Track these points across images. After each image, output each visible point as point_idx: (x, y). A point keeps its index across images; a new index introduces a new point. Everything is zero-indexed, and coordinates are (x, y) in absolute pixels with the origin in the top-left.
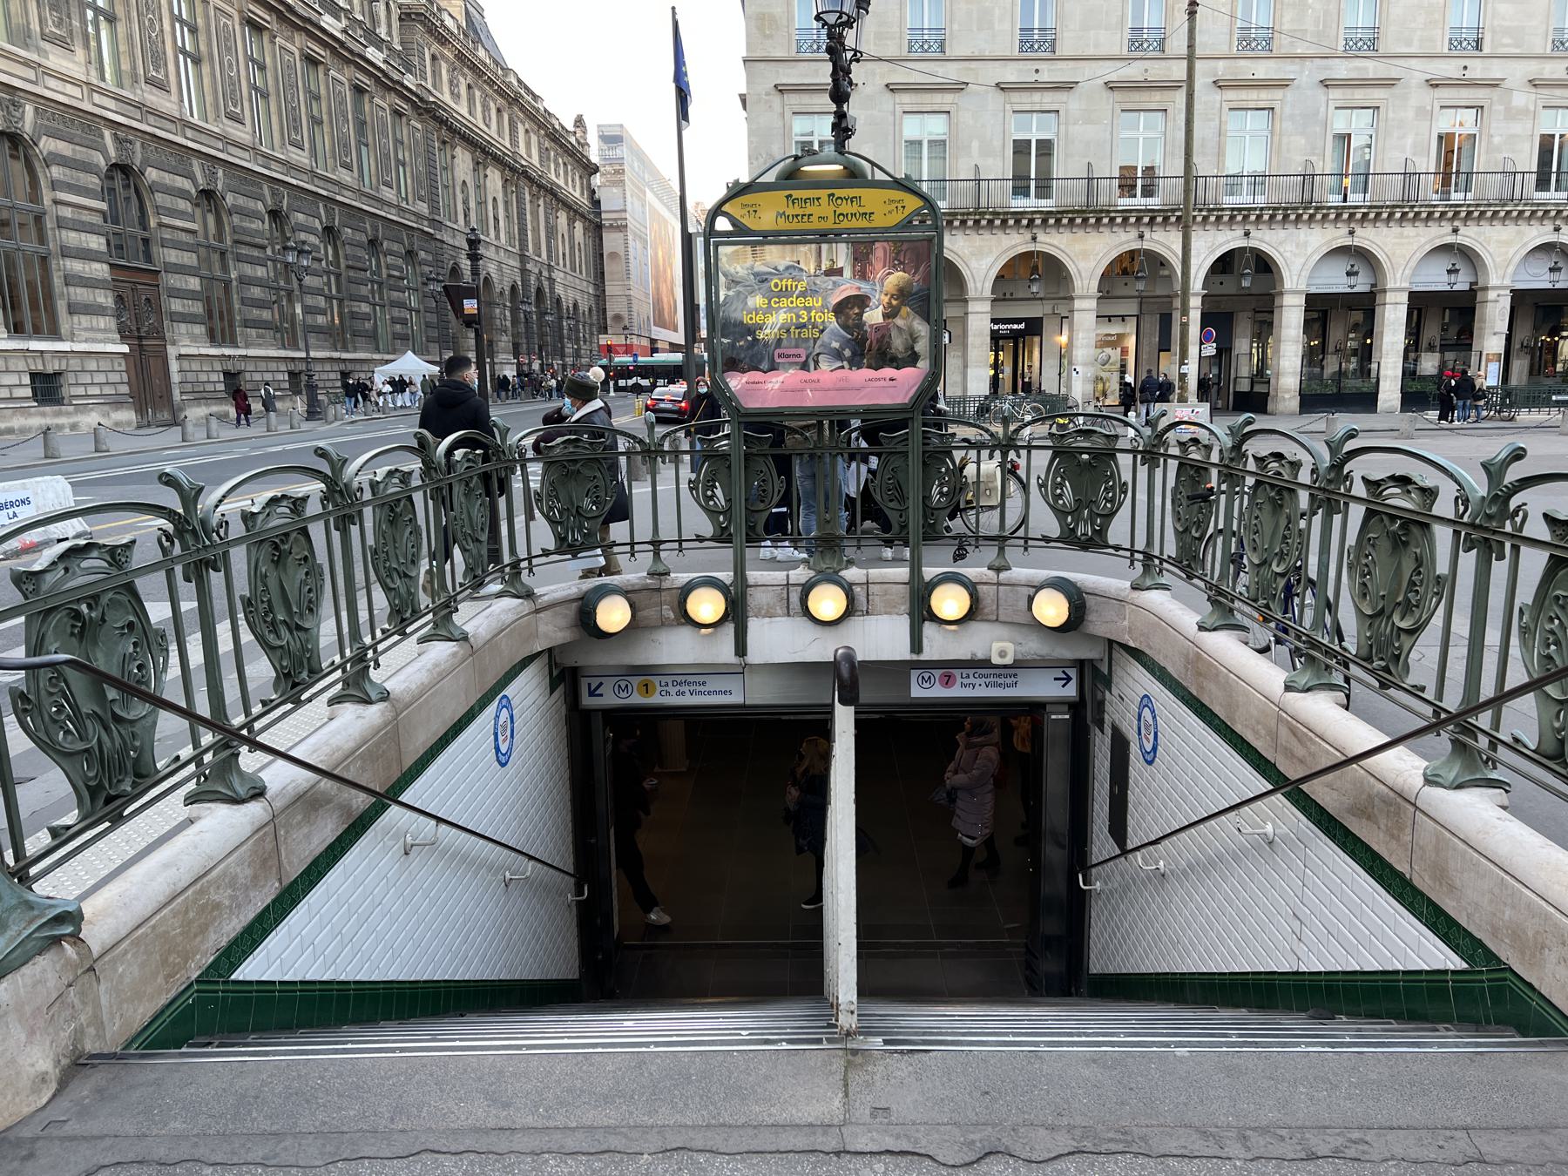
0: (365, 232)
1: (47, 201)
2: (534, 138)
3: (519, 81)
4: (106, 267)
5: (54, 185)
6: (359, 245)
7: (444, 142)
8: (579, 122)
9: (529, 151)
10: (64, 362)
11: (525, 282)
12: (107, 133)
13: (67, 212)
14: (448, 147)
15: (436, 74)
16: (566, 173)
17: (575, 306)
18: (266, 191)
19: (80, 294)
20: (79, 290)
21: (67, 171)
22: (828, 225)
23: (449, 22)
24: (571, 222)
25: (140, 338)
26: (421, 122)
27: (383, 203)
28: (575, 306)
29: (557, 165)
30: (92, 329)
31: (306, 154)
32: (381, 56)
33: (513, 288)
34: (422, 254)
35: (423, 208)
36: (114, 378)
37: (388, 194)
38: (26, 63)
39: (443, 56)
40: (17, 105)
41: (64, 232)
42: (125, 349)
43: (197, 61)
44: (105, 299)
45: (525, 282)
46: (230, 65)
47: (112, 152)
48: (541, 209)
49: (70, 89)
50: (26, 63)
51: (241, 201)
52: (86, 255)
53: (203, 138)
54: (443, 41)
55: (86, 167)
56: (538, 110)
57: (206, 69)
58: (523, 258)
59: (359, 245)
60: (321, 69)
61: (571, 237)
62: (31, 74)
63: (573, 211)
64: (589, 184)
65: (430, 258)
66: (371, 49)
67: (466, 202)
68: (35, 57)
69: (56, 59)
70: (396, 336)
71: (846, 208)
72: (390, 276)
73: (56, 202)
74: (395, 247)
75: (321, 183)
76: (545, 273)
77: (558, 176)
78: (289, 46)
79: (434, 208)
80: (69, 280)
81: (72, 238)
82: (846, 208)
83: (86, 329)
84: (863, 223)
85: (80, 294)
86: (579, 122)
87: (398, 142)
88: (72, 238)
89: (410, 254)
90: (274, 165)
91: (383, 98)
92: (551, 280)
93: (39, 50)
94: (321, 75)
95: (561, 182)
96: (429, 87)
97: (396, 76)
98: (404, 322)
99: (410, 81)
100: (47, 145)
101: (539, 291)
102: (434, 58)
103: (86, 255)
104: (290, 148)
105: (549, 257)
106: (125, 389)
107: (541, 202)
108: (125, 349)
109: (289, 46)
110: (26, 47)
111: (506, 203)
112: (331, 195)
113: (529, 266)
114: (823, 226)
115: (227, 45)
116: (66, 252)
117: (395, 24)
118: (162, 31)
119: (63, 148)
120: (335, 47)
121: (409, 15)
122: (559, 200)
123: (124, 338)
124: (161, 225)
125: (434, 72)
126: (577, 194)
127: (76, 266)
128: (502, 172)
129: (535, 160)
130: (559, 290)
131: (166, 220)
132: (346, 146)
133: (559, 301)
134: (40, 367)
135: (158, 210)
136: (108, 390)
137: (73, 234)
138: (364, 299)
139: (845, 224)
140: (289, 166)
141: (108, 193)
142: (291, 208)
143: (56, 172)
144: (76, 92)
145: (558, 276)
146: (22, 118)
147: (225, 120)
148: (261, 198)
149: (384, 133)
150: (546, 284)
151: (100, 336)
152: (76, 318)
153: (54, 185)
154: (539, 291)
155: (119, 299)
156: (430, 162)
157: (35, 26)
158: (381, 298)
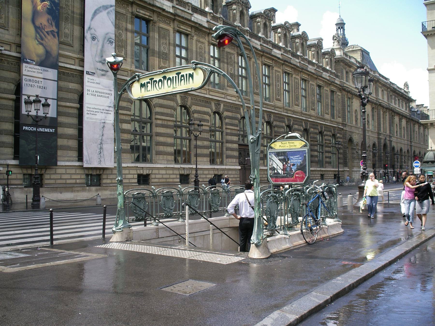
0: (318, 129)
1: (224, 128)
2: (385, 92)
3: (380, 75)
4: (237, 145)
6: (316, 133)
7: (349, 98)
8: (406, 85)
9: (383, 97)
10: (223, 172)
11: (379, 142)
13: (229, 131)
14: (351, 99)
15: (347, 77)
16: (399, 103)
17: (401, 150)
18: (286, 120)
19: (230, 153)
20: (229, 152)
21: (230, 120)
22: (288, 148)
23: (353, 60)
24: (400, 120)
25: (244, 165)
26: (341, 93)
27: (324, 120)
28: (401, 150)
29: (395, 100)
30: (232, 162)
31: (300, 107)
32: (328, 75)
33: (374, 145)
34: (338, 135)
35: (340, 120)
36: (236, 176)
37: (328, 117)
38: (223, 93)
39: (351, 71)
40: (219, 105)
41: (227, 136)
42: (240, 168)
43: (269, 85)
44: (236, 154)
45: (379, 142)
46: (278, 85)
47: (242, 114)
48: (387, 117)
49: (233, 99)
50: (223, 93)
51: (278, 123)
52: (232, 142)
53: (269, 107)
54: (350, 67)
55: (235, 118)
56: (387, 83)
57: (271, 87)
58: (379, 134)
59: (316, 133)
60: (307, 82)
61: (400, 125)
62: (223, 96)
63: (402, 116)
64: (409, 106)
65: (341, 136)
66: (324, 73)
67: (356, 117)
68: (224, 91)
70: (327, 162)
71: (292, 144)
72: (325, 143)
73: (226, 129)
74: (329, 133)
75: (304, 116)
76: (388, 139)
77: (395, 104)
78: (297, 77)
79: (344, 119)
81: (229, 138)
82: (292, 144)
83: (230, 162)
84: (295, 147)
85: (230, 153)
86: (406, 85)
87: (332, 100)
88: (229, 138)
89: (334, 136)
90: (289, 112)
91: (327, 87)
92: (391, 141)
94: (307, 84)
95: (397, 106)
96: (345, 81)
97: (333, 80)
98: (330, 158)
99: (337, 81)
100: (226, 114)
101: (385, 145)
102: (347, 72)
103: (232, 142)
104: (295, 106)
105: (390, 132)
106: (238, 179)
107: (387, 114)
108: (240, 168)
109: (297, 77)
110: (223, 90)
111: (373, 115)
112: (307, 119)
113: (380, 137)
114: (287, 148)
115: (278, 79)
117: (333, 64)
119: (230, 114)
120: (310, 74)
121: (338, 61)
122: (395, 112)
123: (240, 164)
125: (347, 77)
126: (404, 110)
127: (229, 145)
128: (372, 105)
129: (386, 99)
130: (394, 144)
132: (313, 103)
133: (393, 148)
134: (217, 173)
136: (234, 179)
137: (230, 137)
138: (316, 151)
139: (291, 148)
140: (294, 112)
142: (293, 124)
143: (227, 121)
144: (235, 99)
145: (394, 139)
146: (220, 108)
147: (275, 101)
148: (284, 122)
149: (327, 98)
150: (388, 142)
151: (233, 164)
152: (228, 159)
154: (385, 145)
155: (240, 154)
156: (343, 105)
157: (226, 84)
158: (322, 150)
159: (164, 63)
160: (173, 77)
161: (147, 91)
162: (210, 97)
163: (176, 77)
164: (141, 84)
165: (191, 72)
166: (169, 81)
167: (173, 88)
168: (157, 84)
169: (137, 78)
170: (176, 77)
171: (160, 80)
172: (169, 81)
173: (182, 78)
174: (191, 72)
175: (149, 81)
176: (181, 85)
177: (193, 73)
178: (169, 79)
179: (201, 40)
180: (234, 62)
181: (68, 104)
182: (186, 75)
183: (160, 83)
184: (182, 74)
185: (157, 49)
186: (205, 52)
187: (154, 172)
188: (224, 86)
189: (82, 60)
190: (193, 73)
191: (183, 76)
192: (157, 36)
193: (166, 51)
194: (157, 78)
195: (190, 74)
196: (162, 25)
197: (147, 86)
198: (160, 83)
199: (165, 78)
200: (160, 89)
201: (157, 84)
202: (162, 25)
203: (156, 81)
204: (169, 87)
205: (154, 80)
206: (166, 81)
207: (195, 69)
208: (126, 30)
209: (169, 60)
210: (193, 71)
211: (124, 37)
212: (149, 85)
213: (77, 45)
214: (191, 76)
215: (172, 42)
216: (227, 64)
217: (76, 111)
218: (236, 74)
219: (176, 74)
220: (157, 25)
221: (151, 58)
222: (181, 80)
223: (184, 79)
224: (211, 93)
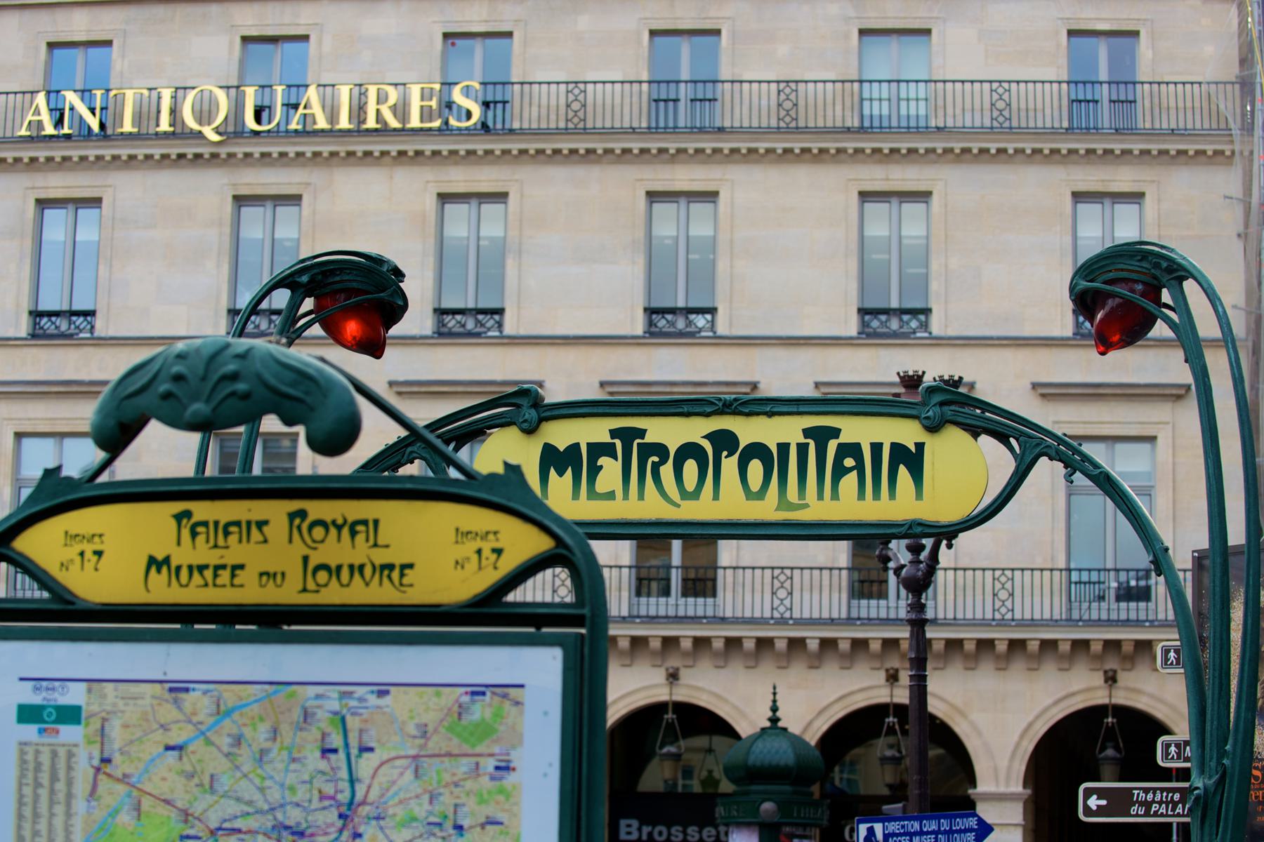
160: (784, 448)
161: (593, 494)
163: (802, 449)
164: (549, 451)
165: (907, 432)
166: (756, 467)
167: (783, 503)
168: (667, 471)
169: (531, 414)
170: (802, 449)
171: (690, 450)
172: (756, 467)
173: (849, 462)
174: (907, 432)
175: (607, 439)
176: (835, 495)
177: (920, 446)
178: (757, 450)
182: (876, 448)
183: (691, 467)
184: (844, 438)
190: (920, 446)
191: (853, 450)
194: (669, 432)
195: (897, 449)
197: (595, 470)
198: (691, 467)
199: (724, 441)
200: (685, 495)
201: (667, 471)
203: (661, 450)
204: (749, 494)
205: (648, 439)
206: (730, 465)
207: (933, 428)
210: (922, 436)
212: (603, 461)
214: (911, 459)
219: (807, 433)
222: (840, 471)
223: (860, 467)
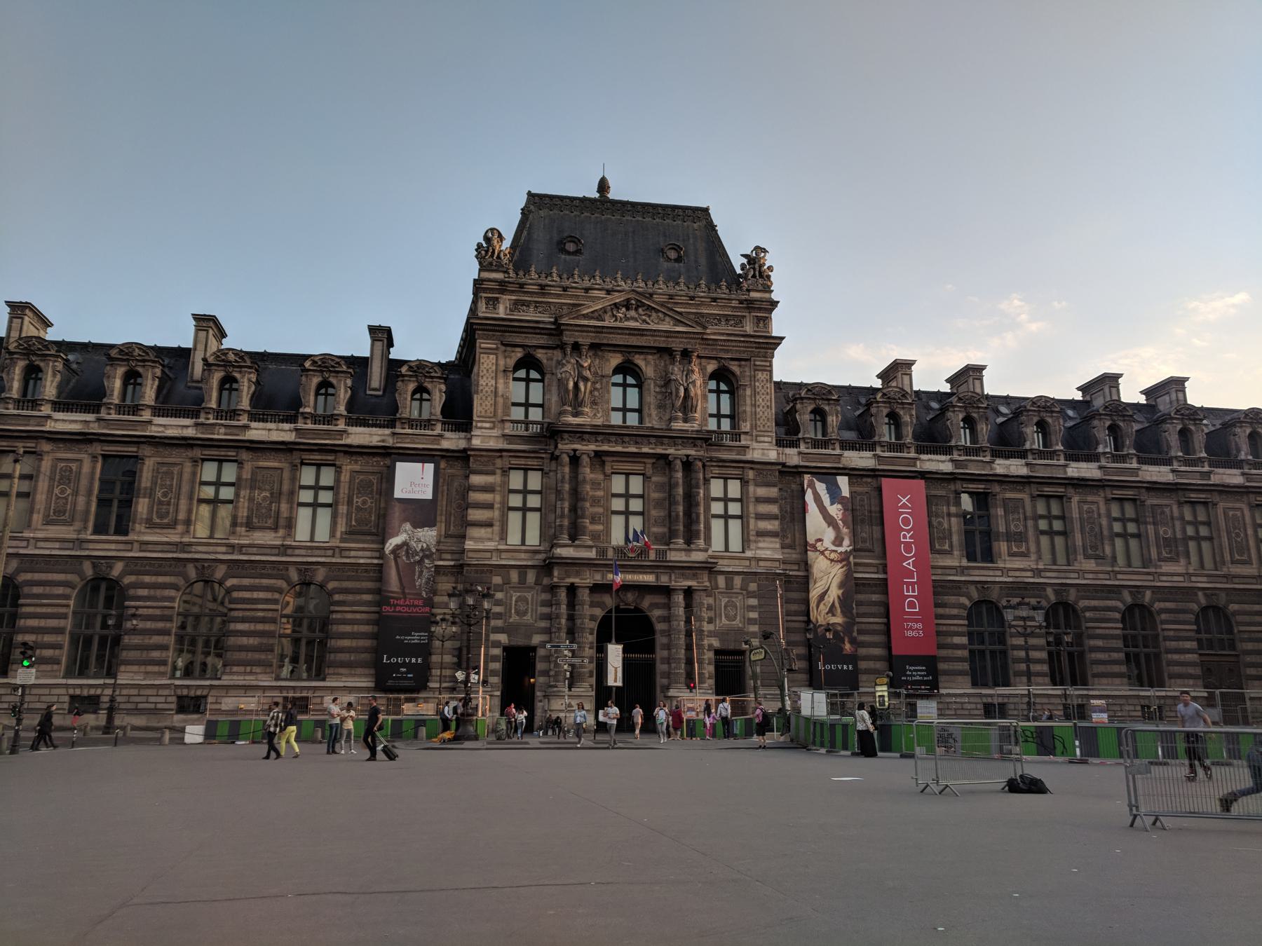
5: (1163, 622)
12: (1200, 594)
38: (1148, 574)
62: (1151, 578)
68: (1153, 570)
69: (1167, 568)
80: (1170, 663)
93: (1156, 567)
100: (1158, 605)
116: (1169, 651)
118: (1246, 535)
124: (1240, 632)
131: (1242, 628)
135: (1239, 624)
141: (1197, 623)
143: (1163, 616)
144: (1181, 579)
153: (1163, 622)
159: (1017, 547)
162: (1117, 583)
179: (1089, 498)
180: (1172, 518)
181: (872, 620)
185: (1002, 529)
186: (1099, 515)
187: (1011, 700)
188: (1151, 561)
189: (885, 566)
192: (1000, 512)
193: (1021, 528)
196: (1008, 495)
202: (1008, 495)
208: (949, 515)
209: (1027, 541)
211: (946, 526)
213: (878, 549)
215: (1029, 513)
216: (1154, 524)
217: (882, 627)
218: (1179, 535)
220: (999, 497)
221: (995, 544)
224: (1119, 576)
